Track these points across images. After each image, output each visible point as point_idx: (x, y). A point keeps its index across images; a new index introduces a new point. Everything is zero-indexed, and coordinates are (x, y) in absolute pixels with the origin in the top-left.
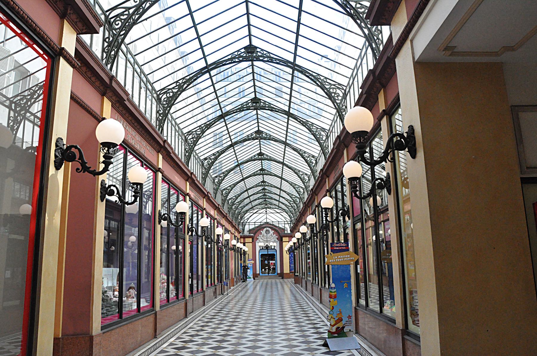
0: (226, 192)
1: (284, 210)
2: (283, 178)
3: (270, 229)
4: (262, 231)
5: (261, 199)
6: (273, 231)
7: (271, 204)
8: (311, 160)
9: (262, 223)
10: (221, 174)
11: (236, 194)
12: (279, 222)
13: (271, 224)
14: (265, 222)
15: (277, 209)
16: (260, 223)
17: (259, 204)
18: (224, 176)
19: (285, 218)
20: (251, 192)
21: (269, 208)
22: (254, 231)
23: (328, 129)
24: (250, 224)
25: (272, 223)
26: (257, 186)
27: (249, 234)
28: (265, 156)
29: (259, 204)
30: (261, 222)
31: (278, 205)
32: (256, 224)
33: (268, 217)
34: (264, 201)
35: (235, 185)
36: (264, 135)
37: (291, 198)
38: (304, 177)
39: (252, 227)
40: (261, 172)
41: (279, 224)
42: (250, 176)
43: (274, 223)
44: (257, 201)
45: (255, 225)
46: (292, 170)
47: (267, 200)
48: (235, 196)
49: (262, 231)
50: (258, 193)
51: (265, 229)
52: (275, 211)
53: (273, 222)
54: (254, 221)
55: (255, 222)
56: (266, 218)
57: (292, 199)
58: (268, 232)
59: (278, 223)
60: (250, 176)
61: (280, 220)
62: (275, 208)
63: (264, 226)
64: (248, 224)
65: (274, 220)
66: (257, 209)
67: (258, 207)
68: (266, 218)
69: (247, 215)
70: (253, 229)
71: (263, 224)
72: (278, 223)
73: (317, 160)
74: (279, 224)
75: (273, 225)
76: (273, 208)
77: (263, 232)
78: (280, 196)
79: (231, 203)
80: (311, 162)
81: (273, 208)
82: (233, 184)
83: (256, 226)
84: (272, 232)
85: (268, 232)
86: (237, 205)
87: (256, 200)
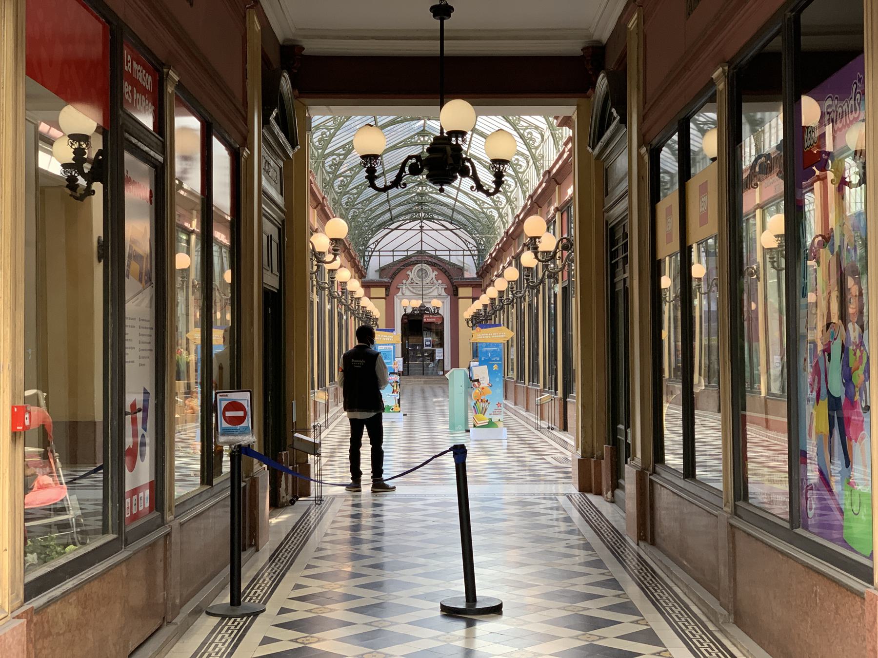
2: (461, 190)
3: (426, 267)
4: (409, 273)
6: (436, 273)
9: (410, 253)
12: (450, 250)
13: (431, 256)
14: (418, 251)
16: (405, 253)
19: (465, 242)
21: (428, 219)
22: (392, 271)
25: (433, 253)
27: (380, 277)
30: (407, 251)
32: (395, 253)
33: (425, 238)
39: (387, 261)
41: (450, 255)
43: (438, 253)
45: (393, 256)
49: (409, 273)
51: (417, 267)
52: (443, 226)
53: (436, 250)
54: (391, 247)
55: (393, 251)
58: (422, 274)
59: (447, 253)
61: (452, 246)
63: (413, 259)
65: (439, 247)
66: (403, 220)
68: (421, 241)
71: (411, 256)
75: (436, 257)
76: (438, 220)
77: (413, 273)
78: (456, 200)
81: (438, 220)
83: (396, 259)
84: (432, 274)
85: (422, 274)
87: (400, 205)
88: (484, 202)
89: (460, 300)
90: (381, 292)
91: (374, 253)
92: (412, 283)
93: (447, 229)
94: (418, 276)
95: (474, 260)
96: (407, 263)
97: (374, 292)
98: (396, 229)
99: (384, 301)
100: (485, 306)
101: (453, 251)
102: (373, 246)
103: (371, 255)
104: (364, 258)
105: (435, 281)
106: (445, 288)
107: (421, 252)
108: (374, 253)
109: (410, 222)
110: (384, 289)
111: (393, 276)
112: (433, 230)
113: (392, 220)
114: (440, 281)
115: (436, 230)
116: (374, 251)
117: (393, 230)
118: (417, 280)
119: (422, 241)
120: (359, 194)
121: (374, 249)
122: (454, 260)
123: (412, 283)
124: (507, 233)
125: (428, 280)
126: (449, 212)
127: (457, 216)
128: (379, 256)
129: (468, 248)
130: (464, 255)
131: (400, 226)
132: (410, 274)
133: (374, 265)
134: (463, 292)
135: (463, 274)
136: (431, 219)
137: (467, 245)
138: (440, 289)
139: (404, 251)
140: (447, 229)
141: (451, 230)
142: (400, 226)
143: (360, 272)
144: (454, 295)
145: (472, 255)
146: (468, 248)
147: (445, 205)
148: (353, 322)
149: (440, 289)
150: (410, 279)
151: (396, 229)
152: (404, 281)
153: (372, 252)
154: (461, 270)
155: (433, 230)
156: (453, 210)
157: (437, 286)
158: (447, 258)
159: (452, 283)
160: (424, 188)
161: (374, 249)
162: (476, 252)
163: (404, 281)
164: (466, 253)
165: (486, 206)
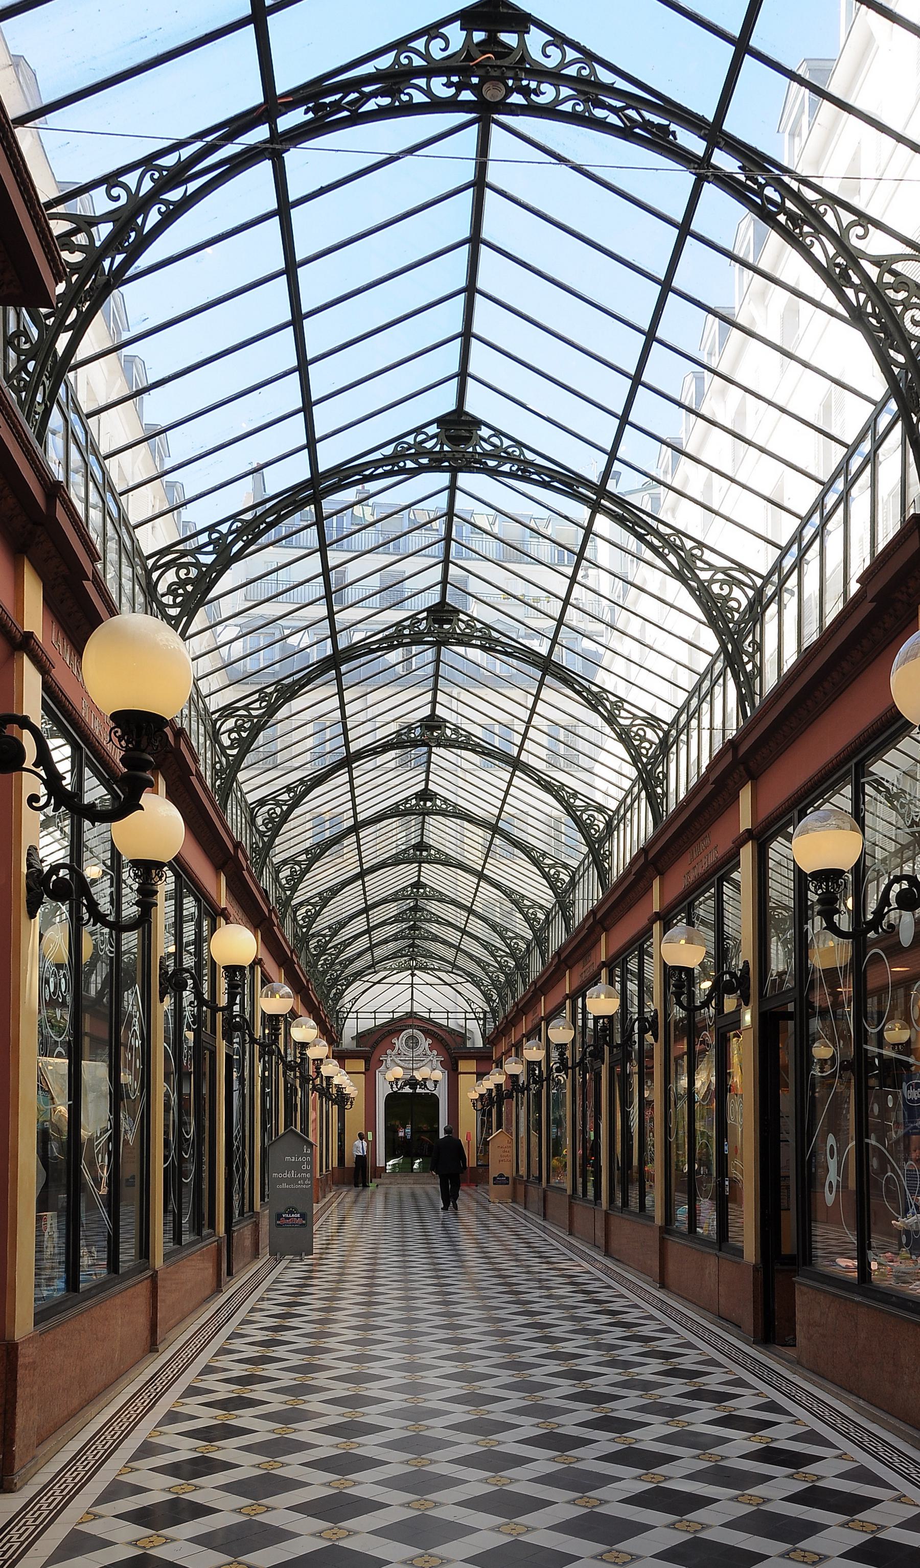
0: (306, 912)
1: (469, 974)
5: (403, 938)
7: (430, 955)
8: (559, 875)
9: (396, 1015)
10: (300, 854)
11: (332, 921)
12: (448, 1012)
13: (422, 1019)
14: (407, 1013)
15: (447, 972)
16: (391, 1015)
17: (394, 956)
18: (308, 859)
20: (377, 915)
21: (420, 969)
23: (614, 809)
24: (360, 1015)
25: (427, 1015)
26: (395, 898)
28: (433, 852)
29: (394, 956)
30: (393, 1012)
31: (452, 959)
32: (378, 1015)
34: (409, 946)
35: (334, 891)
36: (438, 802)
37: (494, 957)
38: (536, 915)
39: (366, 1024)
40: (418, 853)
41: (448, 1018)
42: (382, 865)
44: (391, 945)
45: (375, 1018)
46: (504, 893)
47: (417, 942)
48: (330, 927)
50: (395, 938)
51: (404, 1035)
55: (375, 1012)
56: (412, 999)
57: (497, 961)
58: (413, 1042)
59: (445, 1015)
60: (382, 865)
62: (439, 970)
64: (355, 1015)
67: (390, 964)
69: (356, 987)
70: (369, 1032)
72: (445, 1015)
73: (574, 875)
74: (448, 1018)
75: (430, 1019)
77: (399, 1042)
79: (315, 948)
80: (557, 880)
82: (329, 889)
83: (379, 1022)
85: (413, 1042)
86: (330, 954)
88: (489, 965)
89: (461, 1076)
90: (360, 1065)
91: (350, 1015)
92: (399, 1054)
93: (447, 984)
94: (407, 1045)
95: (479, 1024)
96: (394, 1027)
97: (350, 1064)
98: (379, 982)
99: (363, 1076)
100: (490, 1090)
101: (452, 1013)
102: (348, 1006)
103: (347, 1018)
104: (337, 1021)
105: (429, 1052)
106: (441, 1061)
107: (411, 1015)
108: (350, 1014)
109: (398, 973)
110: (362, 1062)
111: (376, 1044)
112: (428, 984)
113: (372, 966)
114: (435, 1052)
115: (431, 985)
116: (350, 1012)
117: (375, 984)
118: (404, 1049)
119: (412, 999)
120: (333, 936)
121: (351, 1008)
122: (452, 1024)
123: (399, 1054)
124: (516, 1004)
125: (419, 1051)
126: (449, 954)
127: (462, 961)
128: (357, 1018)
129: (472, 1009)
130: (466, 1019)
131: (384, 978)
132: (396, 1042)
133: (350, 1029)
134: (463, 1066)
135: (465, 1043)
136: (424, 969)
137: (470, 1006)
138: (434, 1062)
139: (389, 1012)
140: (447, 984)
141: (450, 985)
142: (384, 978)
143: (330, 1033)
144: (453, 1070)
145: (477, 1019)
146: (472, 1009)
147: (444, 942)
148: (318, 1102)
149: (434, 1062)
150: (397, 1048)
151: (379, 982)
152: (389, 1052)
153: (348, 1013)
154: (462, 1036)
155: (428, 984)
156: (464, 932)
157: (431, 1058)
158: (444, 1022)
159: (450, 1055)
160: (422, 891)
161: (351, 1008)
162: (482, 1016)
163: (389, 1052)
164: (468, 1016)
165: (491, 969)
